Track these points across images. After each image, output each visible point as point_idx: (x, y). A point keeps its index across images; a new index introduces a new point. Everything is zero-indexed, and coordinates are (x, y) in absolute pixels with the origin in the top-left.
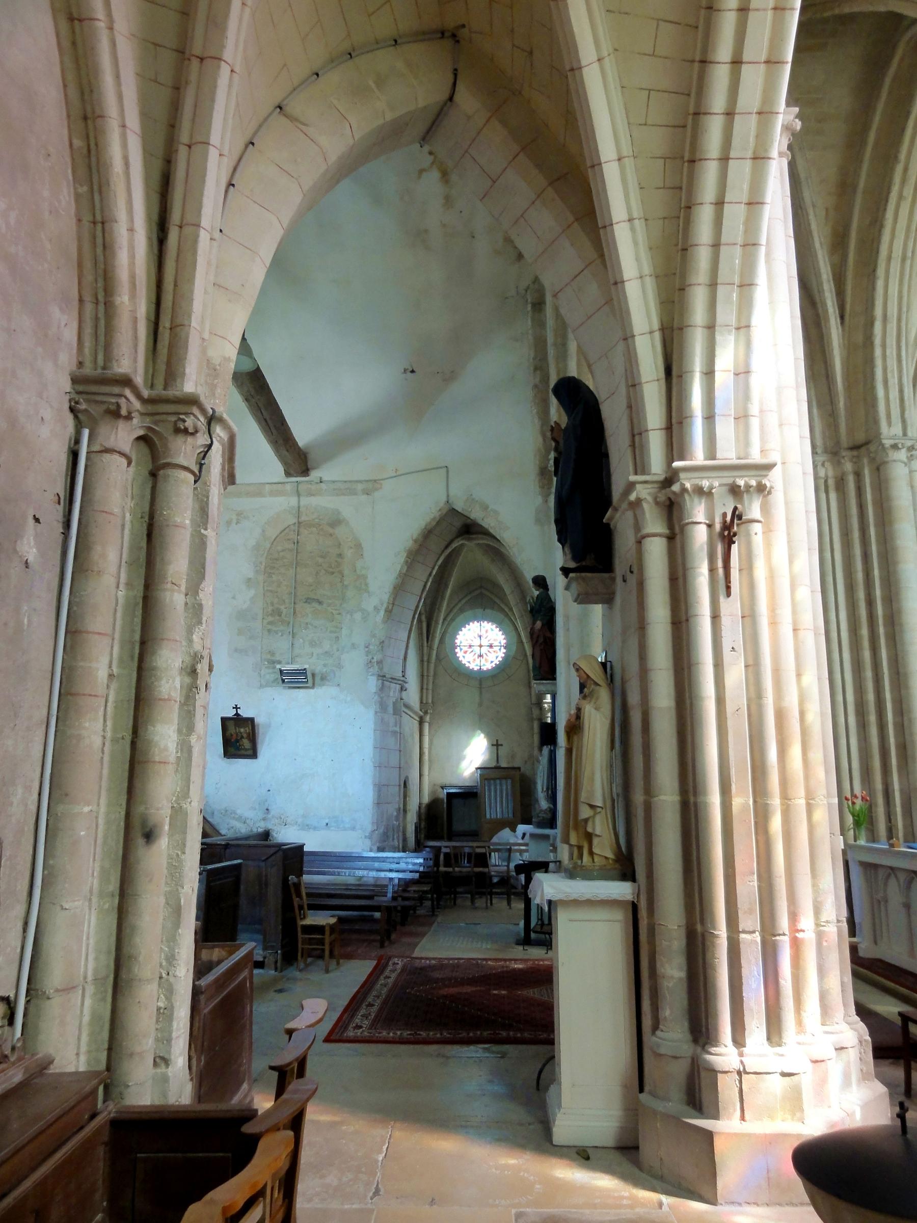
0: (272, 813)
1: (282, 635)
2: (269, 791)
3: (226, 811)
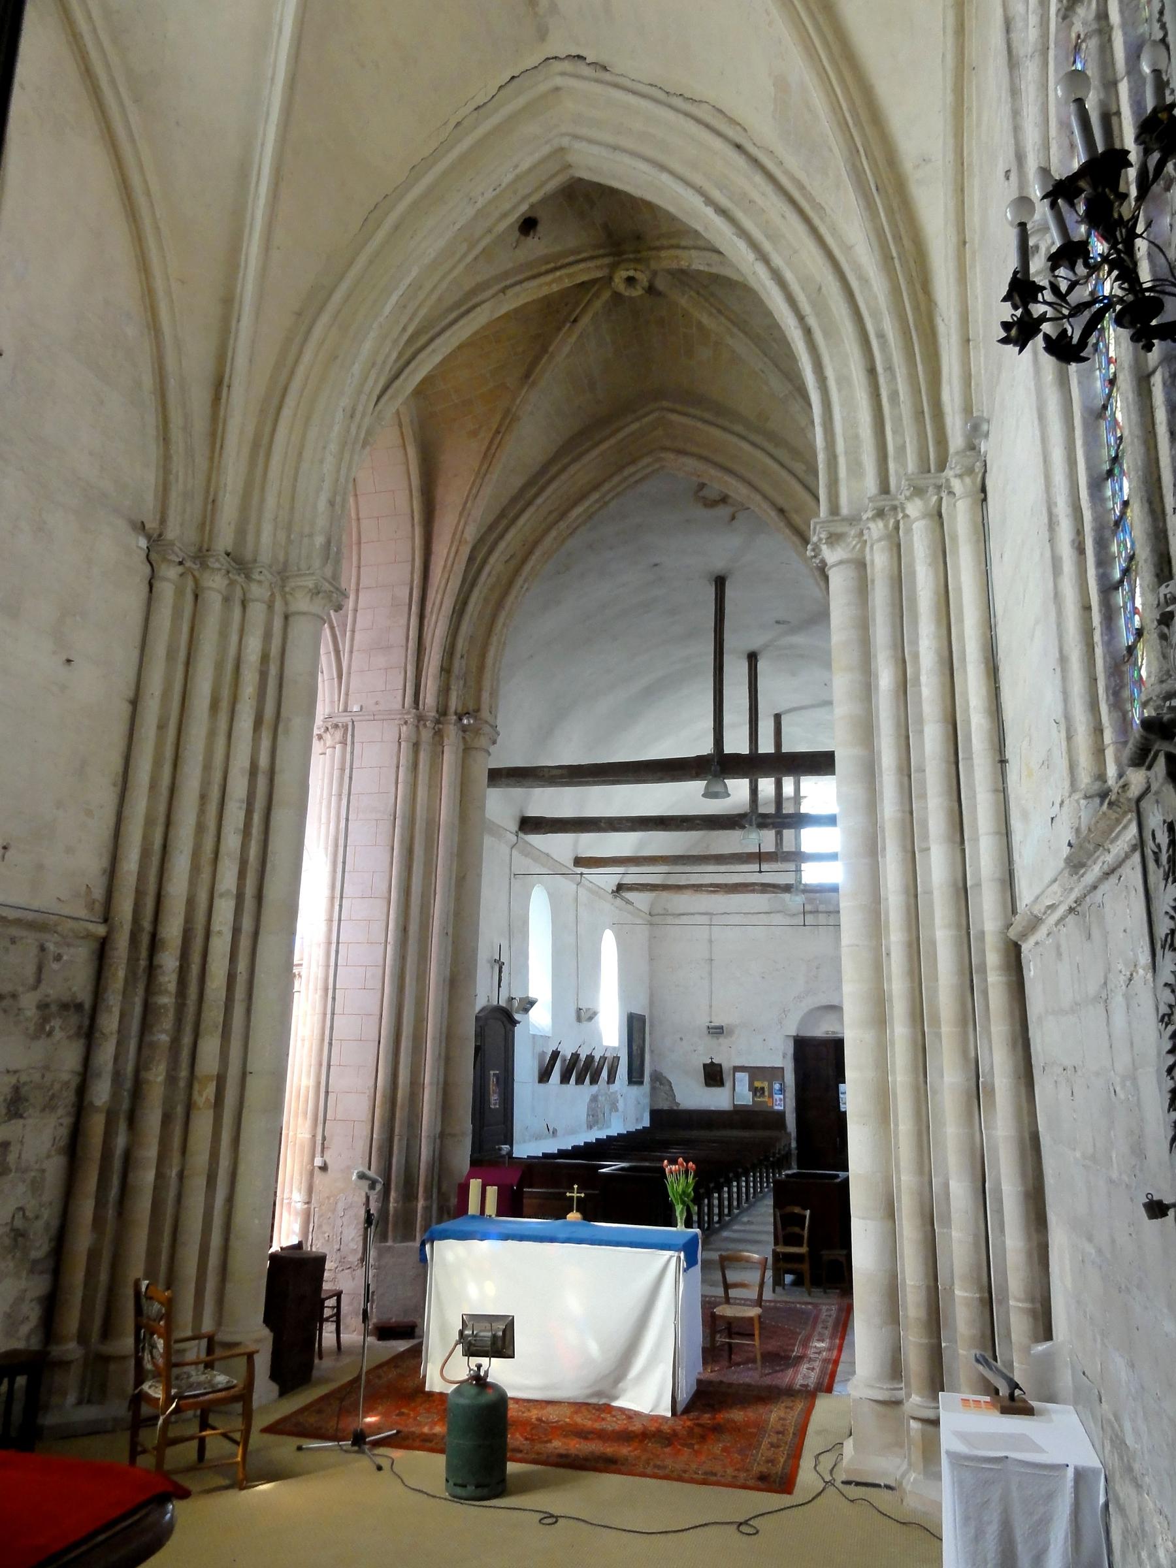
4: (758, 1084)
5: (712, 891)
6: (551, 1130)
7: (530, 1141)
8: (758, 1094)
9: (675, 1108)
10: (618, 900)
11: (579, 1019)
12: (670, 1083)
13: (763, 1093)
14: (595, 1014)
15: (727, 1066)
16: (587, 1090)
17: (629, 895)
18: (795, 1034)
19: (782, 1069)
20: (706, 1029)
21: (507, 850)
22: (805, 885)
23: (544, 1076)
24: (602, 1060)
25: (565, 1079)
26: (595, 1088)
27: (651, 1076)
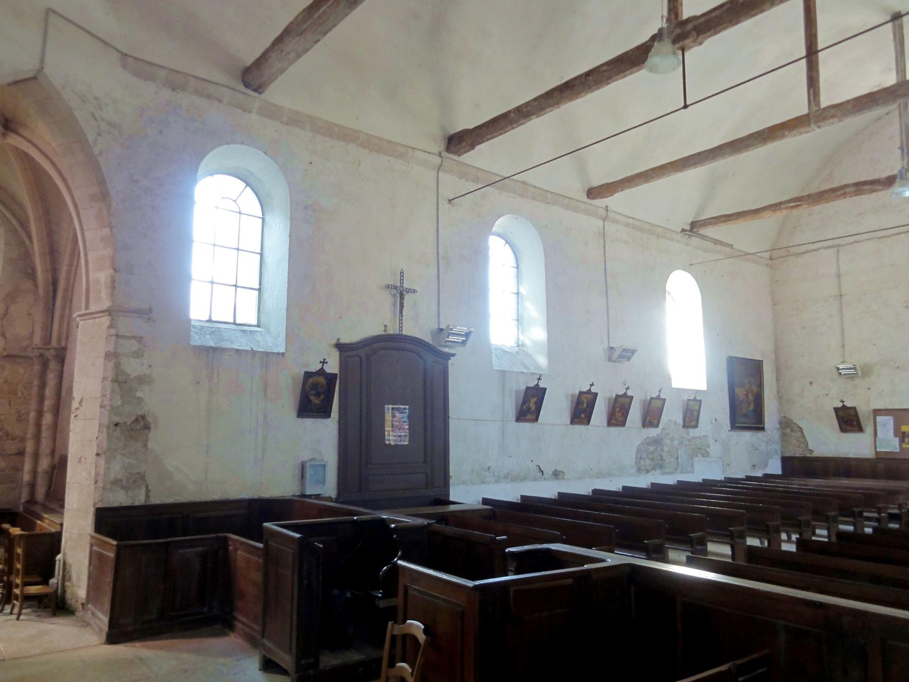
5: (792, 207)
9: (809, 455)
10: (695, 241)
11: (610, 359)
15: (864, 410)
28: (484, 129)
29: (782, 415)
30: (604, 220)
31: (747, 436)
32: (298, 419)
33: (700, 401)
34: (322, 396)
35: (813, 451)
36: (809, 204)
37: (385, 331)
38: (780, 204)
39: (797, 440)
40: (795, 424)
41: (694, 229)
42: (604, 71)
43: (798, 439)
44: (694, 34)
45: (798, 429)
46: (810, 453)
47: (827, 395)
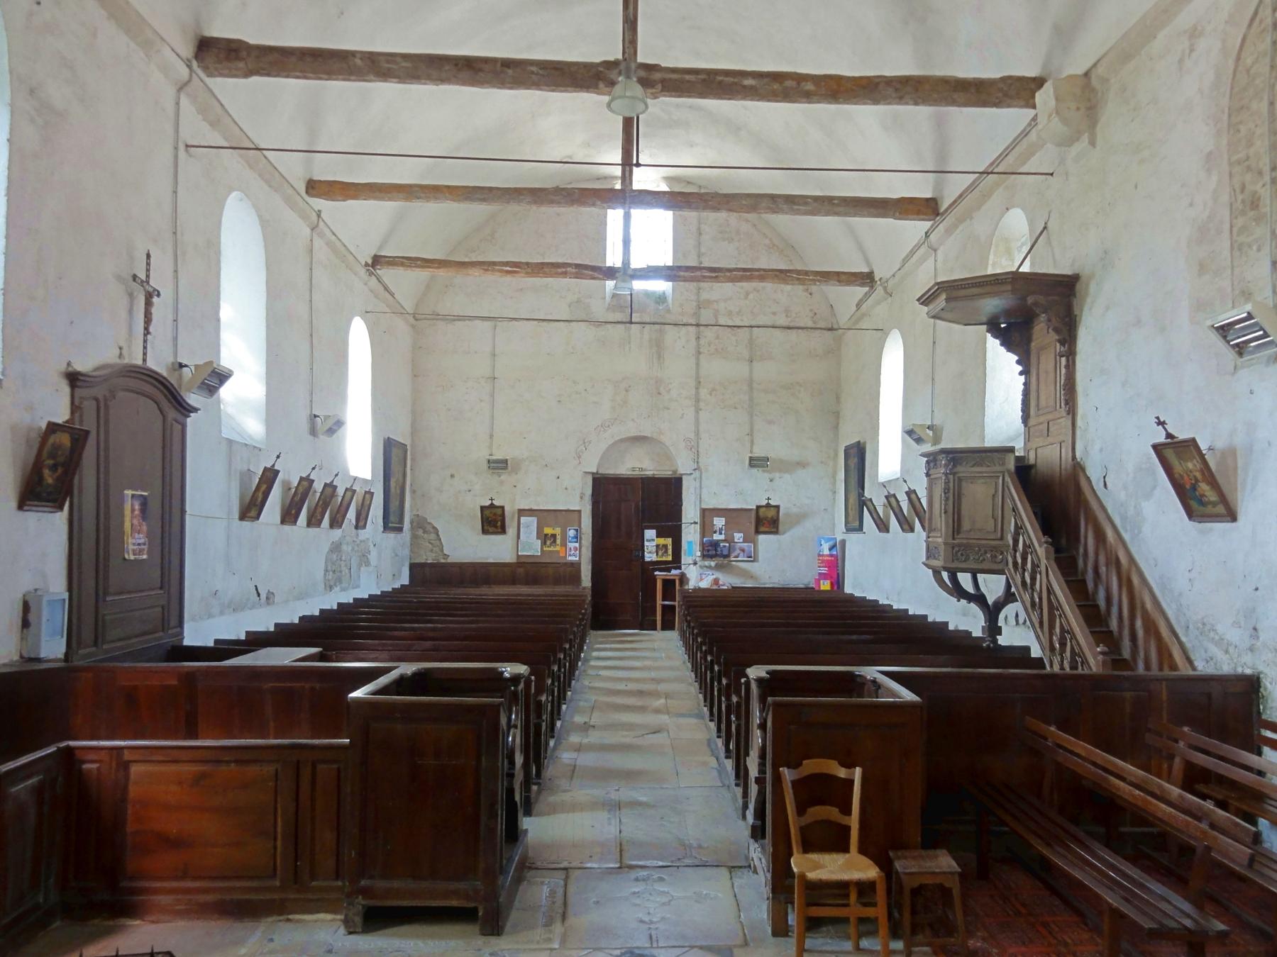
0: (1263, 636)
1: (1259, 250)
2: (1257, 589)
3: (1204, 624)
4: (548, 531)
5: (508, 272)
6: (263, 596)
7: (222, 613)
8: (548, 543)
9: (443, 561)
11: (313, 432)
12: (436, 531)
13: (555, 541)
14: (339, 424)
16: (325, 535)
17: (385, 273)
18: (595, 471)
19: (579, 511)
20: (486, 462)
21: (170, 91)
22: (635, 270)
23: (251, 508)
24: (349, 494)
25: (289, 516)
26: (337, 533)
27: (412, 523)
28: (293, 59)
29: (415, 513)
30: (312, 230)
31: (392, 535)
32: (21, 513)
33: (373, 493)
34: (60, 470)
35: (448, 556)
36: (527, 273)
37: (121, 356)
38: (494, 263)
39: (430, 543)
40: (429, 523)
41: (377, 265)
42: (533, 73)
43: (431, 541)
44: (659, 86)
45: (431, 530)
46: (444, 559)
47: (470, 491)
